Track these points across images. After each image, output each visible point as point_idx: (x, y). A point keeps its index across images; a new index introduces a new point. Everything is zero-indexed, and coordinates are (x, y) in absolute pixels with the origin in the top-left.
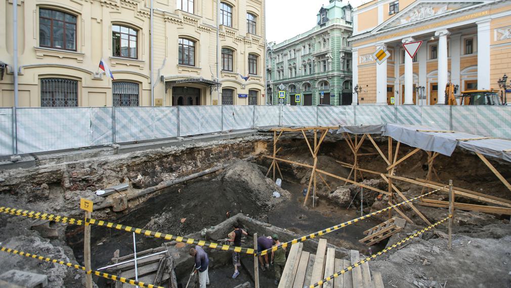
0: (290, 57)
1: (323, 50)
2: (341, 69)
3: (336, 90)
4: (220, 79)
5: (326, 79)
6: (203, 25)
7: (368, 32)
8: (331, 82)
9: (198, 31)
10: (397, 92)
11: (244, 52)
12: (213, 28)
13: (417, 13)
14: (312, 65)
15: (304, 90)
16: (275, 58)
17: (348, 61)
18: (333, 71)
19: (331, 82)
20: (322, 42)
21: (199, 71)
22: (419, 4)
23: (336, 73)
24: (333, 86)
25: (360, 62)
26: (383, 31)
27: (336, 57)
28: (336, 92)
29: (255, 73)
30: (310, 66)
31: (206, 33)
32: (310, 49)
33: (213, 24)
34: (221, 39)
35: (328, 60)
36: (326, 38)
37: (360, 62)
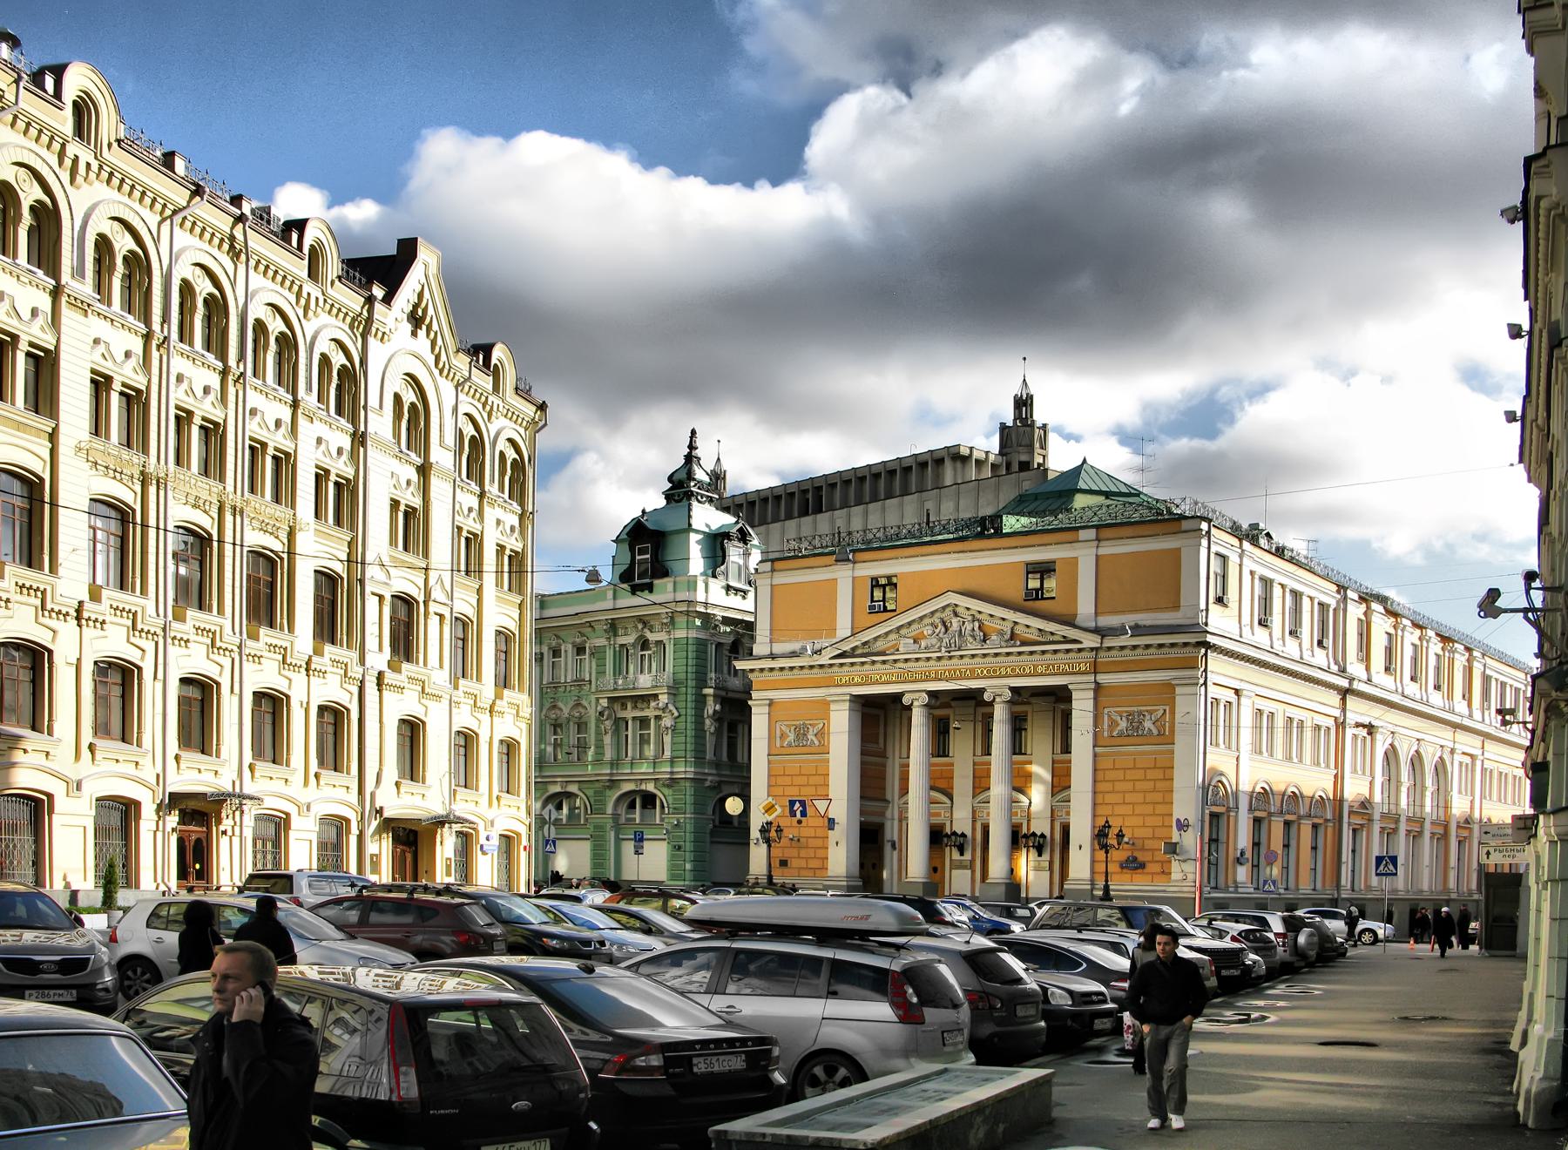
5: (650, 787)
17: (732, 728)
35: (658, 718)
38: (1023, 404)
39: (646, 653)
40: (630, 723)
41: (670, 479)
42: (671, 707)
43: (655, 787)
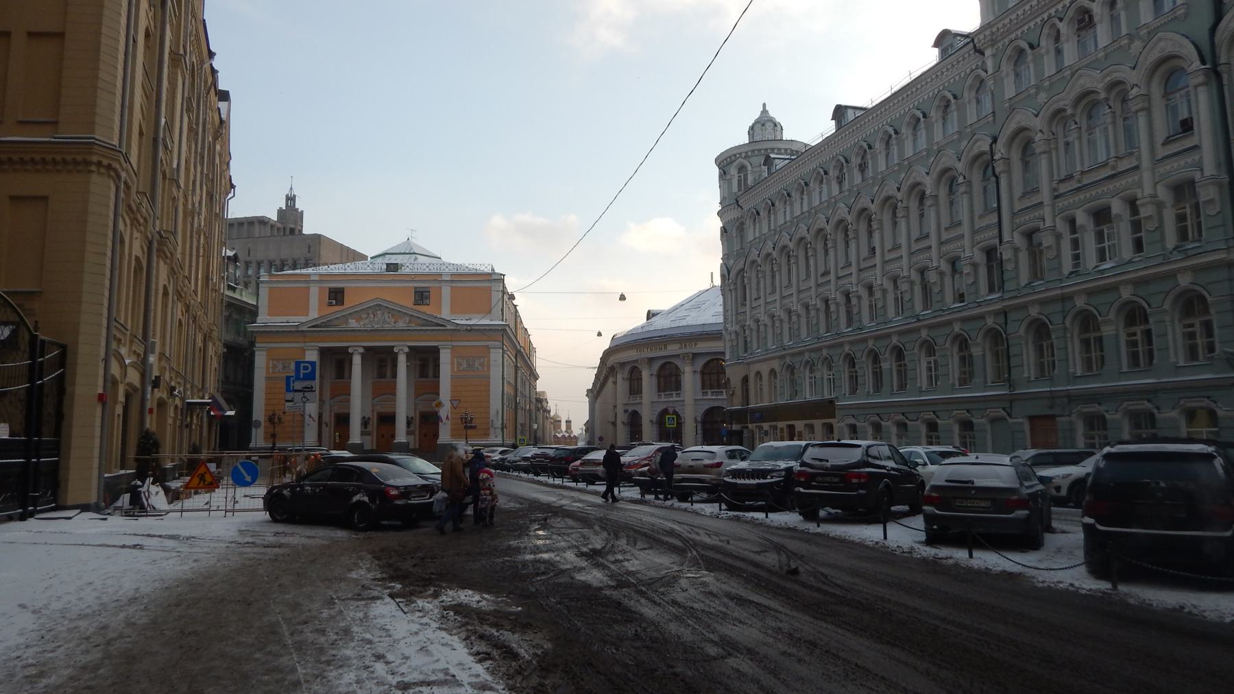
13: (371, 316)
25: (271, 371)
26: (318, 328)
37: (271, 371)
38: (291, 199)
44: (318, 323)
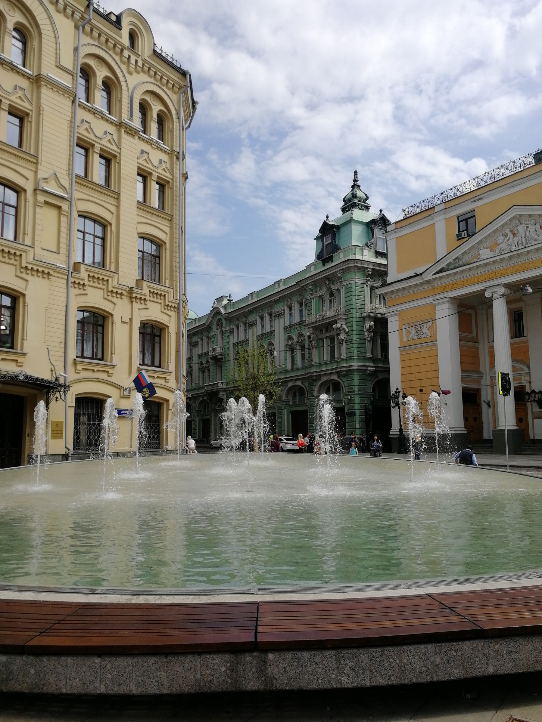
0: (262, 329)
1: (329, 313)
2: (369, 355)
3: (357, 401)
4: (71, 376)
5: (335, 377)
6: (35, 262)
7: (416, 275)
8: (346, 384)
9: (24, 275)
10: (489, 404)
11: (131, 319)
12: (58, 270)
14: (307, 346)
15: (291, 403)
16: (231, 332)
18: (347, 360)
19: (346, 384)
20: (327, 298)
21: (20, 360)
22: (514, 217)
23: (355, 364)
24: (351, 392)
27: (355, 328)
28: (357, 406)
29: (157, 363)
30: (303, 348)
31: (40, 279)
32: (301, 311)
33: (60, 262)
34: (77, 291)
35: (338, 335)
36: (334, 287)
37: (405, 340)
39: (332, 298)
40: (325, 340)
41: (344, 200)
42: (344, 326)
43: (338, 377)
44: (443, 265)
